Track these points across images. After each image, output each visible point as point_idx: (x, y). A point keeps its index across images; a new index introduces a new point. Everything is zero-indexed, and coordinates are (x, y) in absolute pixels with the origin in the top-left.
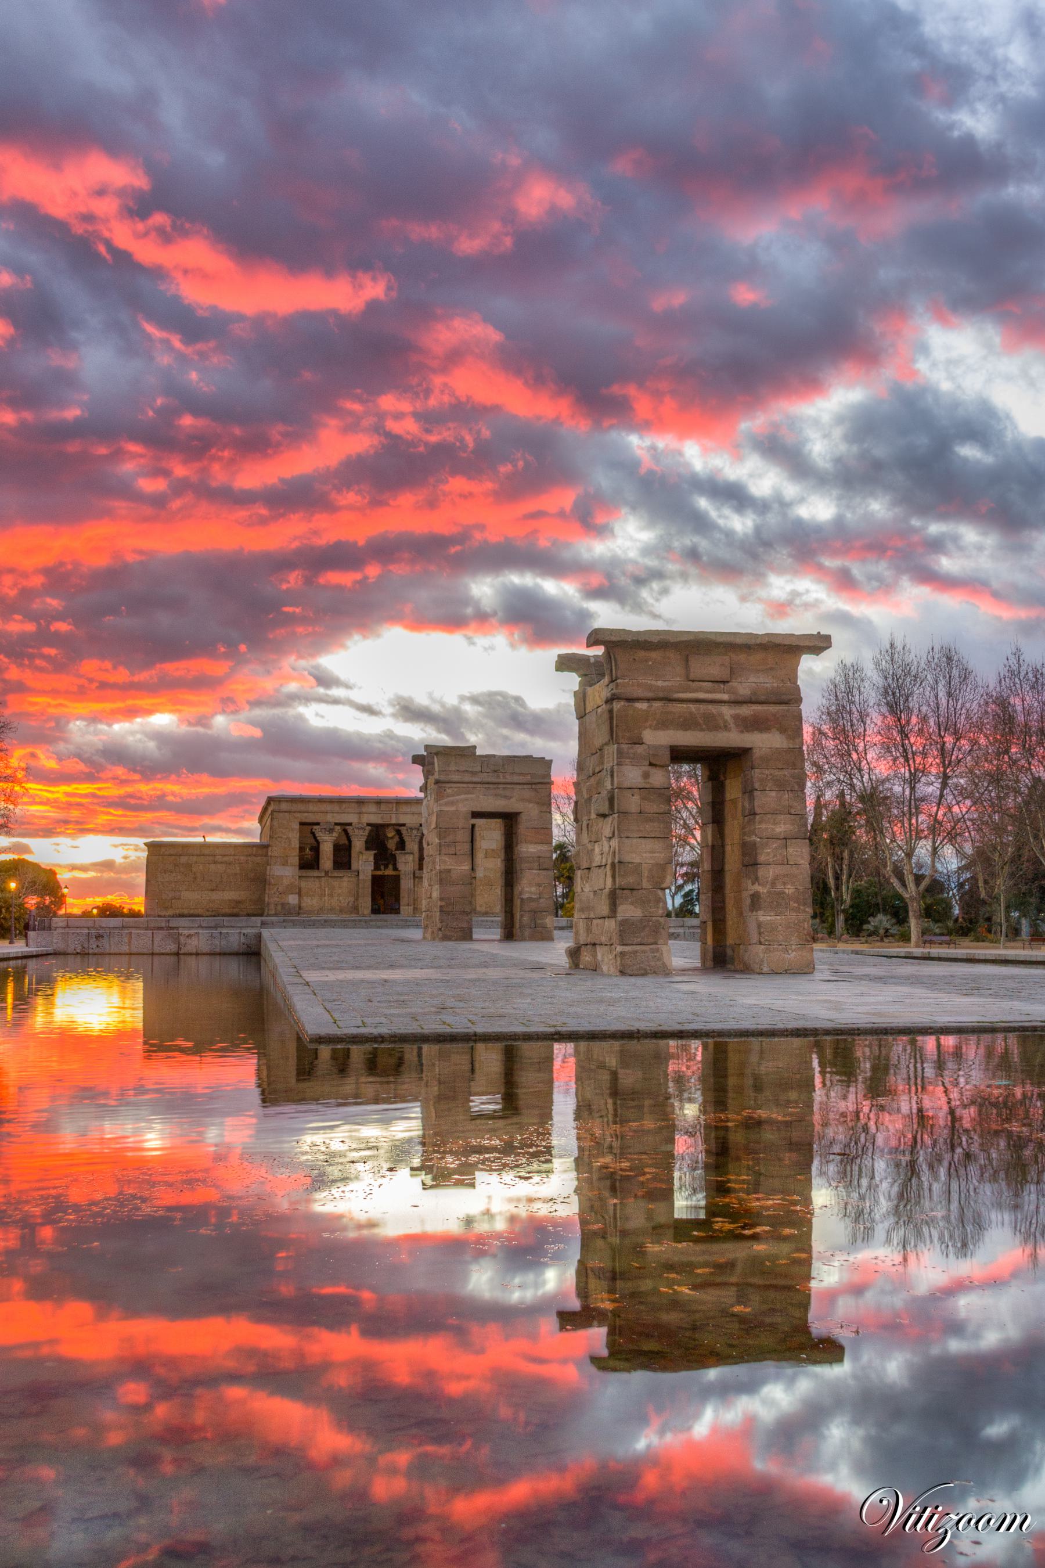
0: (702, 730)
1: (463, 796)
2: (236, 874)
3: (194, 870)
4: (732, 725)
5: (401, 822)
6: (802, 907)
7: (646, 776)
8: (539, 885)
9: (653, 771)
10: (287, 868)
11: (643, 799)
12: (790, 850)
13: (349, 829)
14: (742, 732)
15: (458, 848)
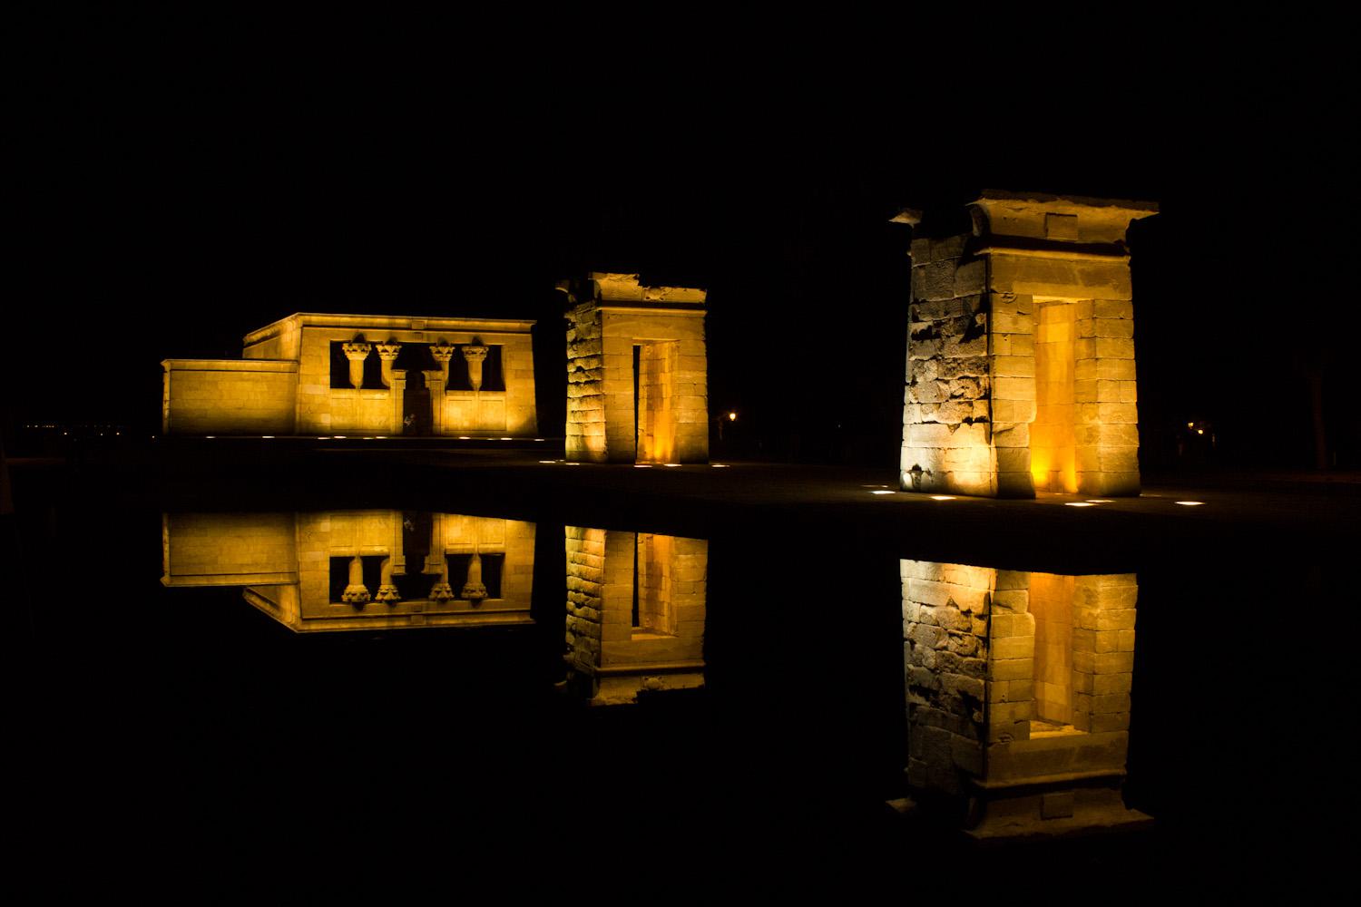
0: (1058, 283)
1: (624, 324)
2: (262, 393)
3: (220, 388)
4: (1080, 281)
5: (433, 342)
6: (1131, 440)
7: (1015, 322)
8: (694, 410)
9: (1021, 318)
10: (320, 386)
11: (1013, 343)
12: (1122, 390)
13: (380, 348)
14: (1086, 285)
15: (621, 373)
